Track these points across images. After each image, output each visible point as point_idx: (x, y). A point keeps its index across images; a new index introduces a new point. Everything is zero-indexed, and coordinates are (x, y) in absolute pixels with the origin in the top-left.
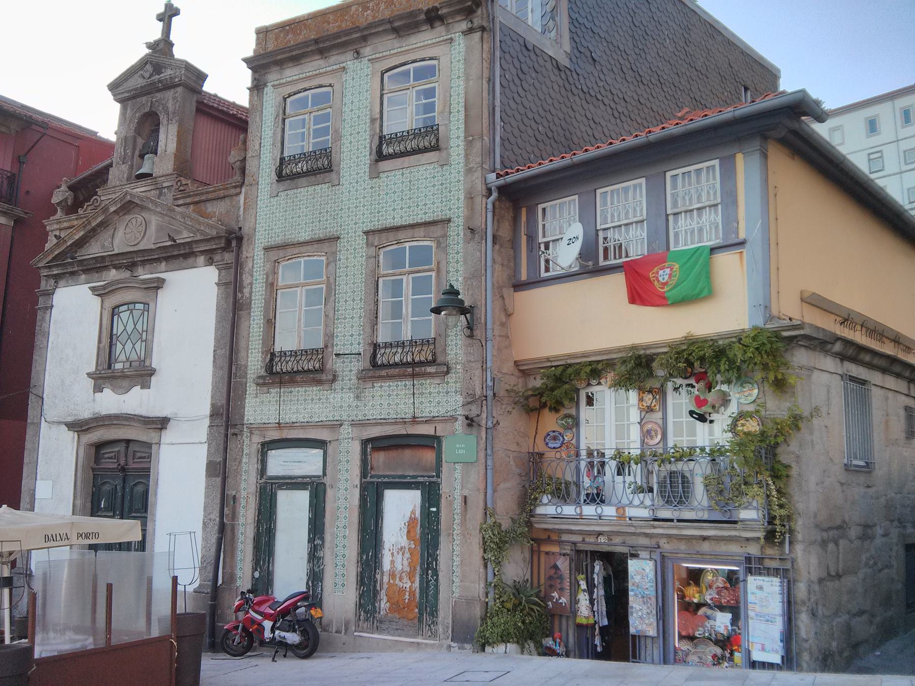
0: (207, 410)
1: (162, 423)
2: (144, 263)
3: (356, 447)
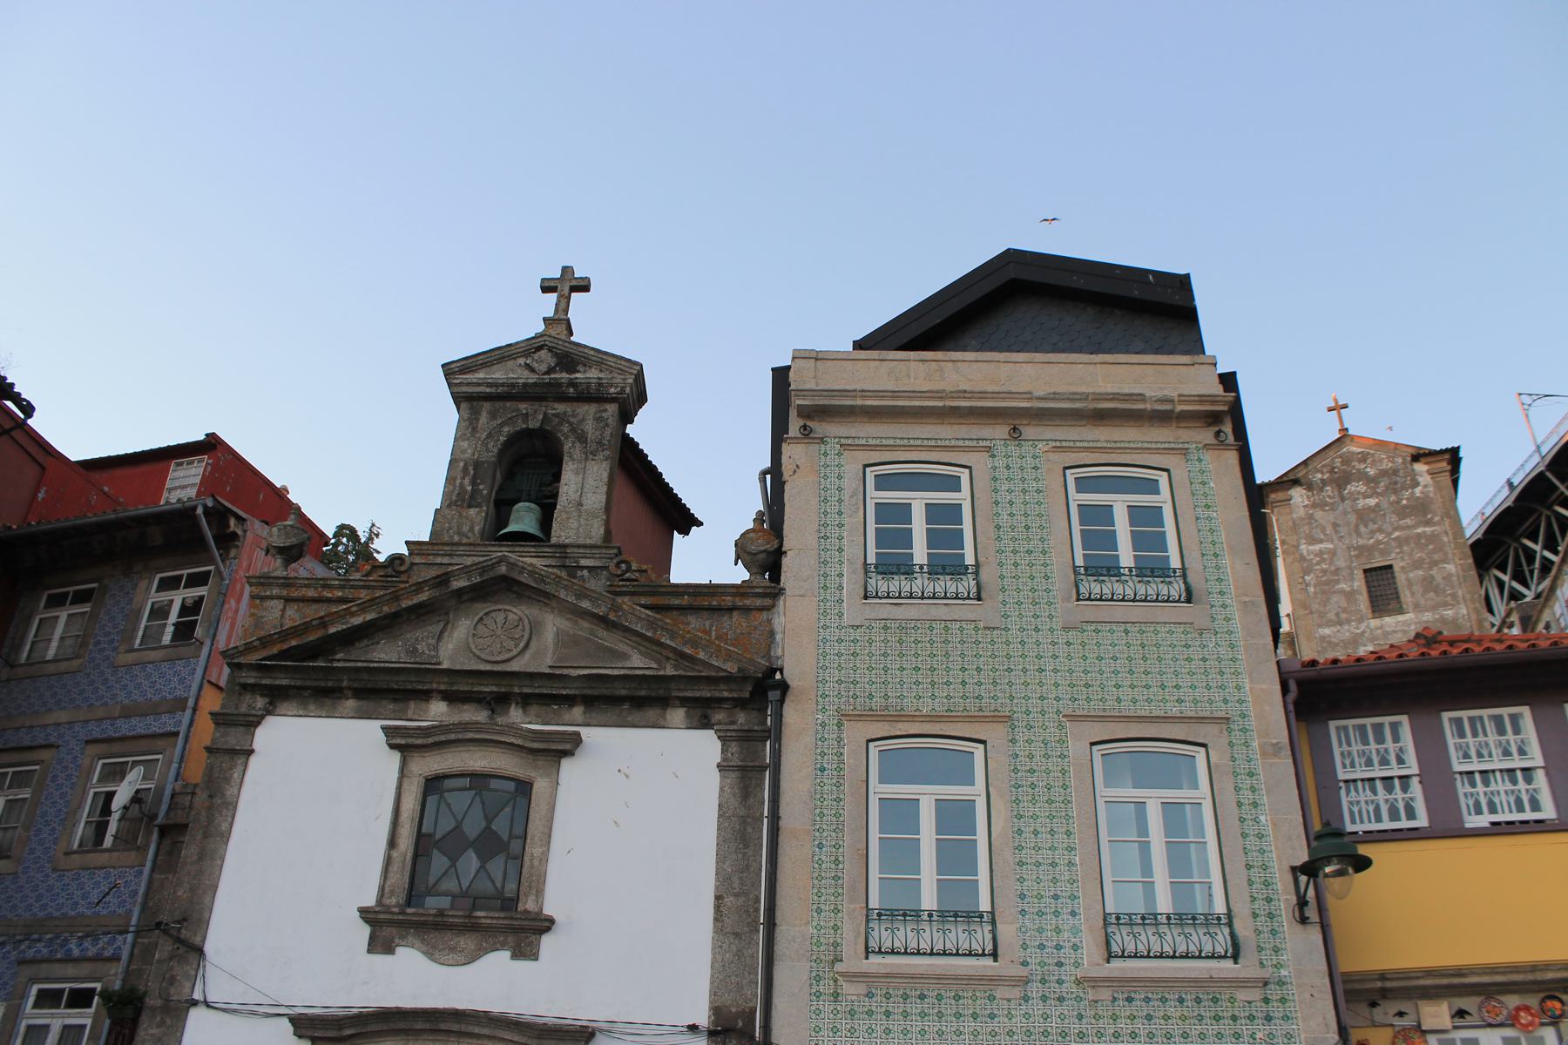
2: (526, 701)
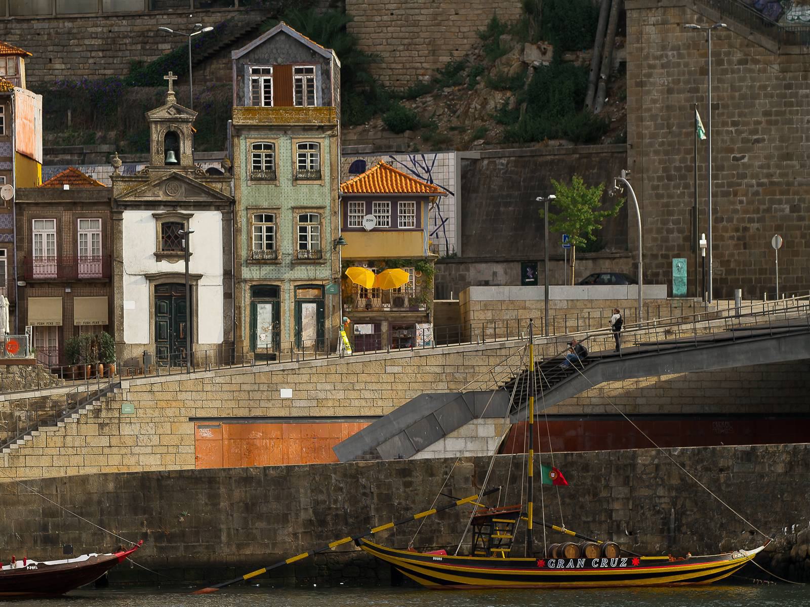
0: (221, 272)
1: (200, 277)
2: (181, 206)
3: (292, 287)
